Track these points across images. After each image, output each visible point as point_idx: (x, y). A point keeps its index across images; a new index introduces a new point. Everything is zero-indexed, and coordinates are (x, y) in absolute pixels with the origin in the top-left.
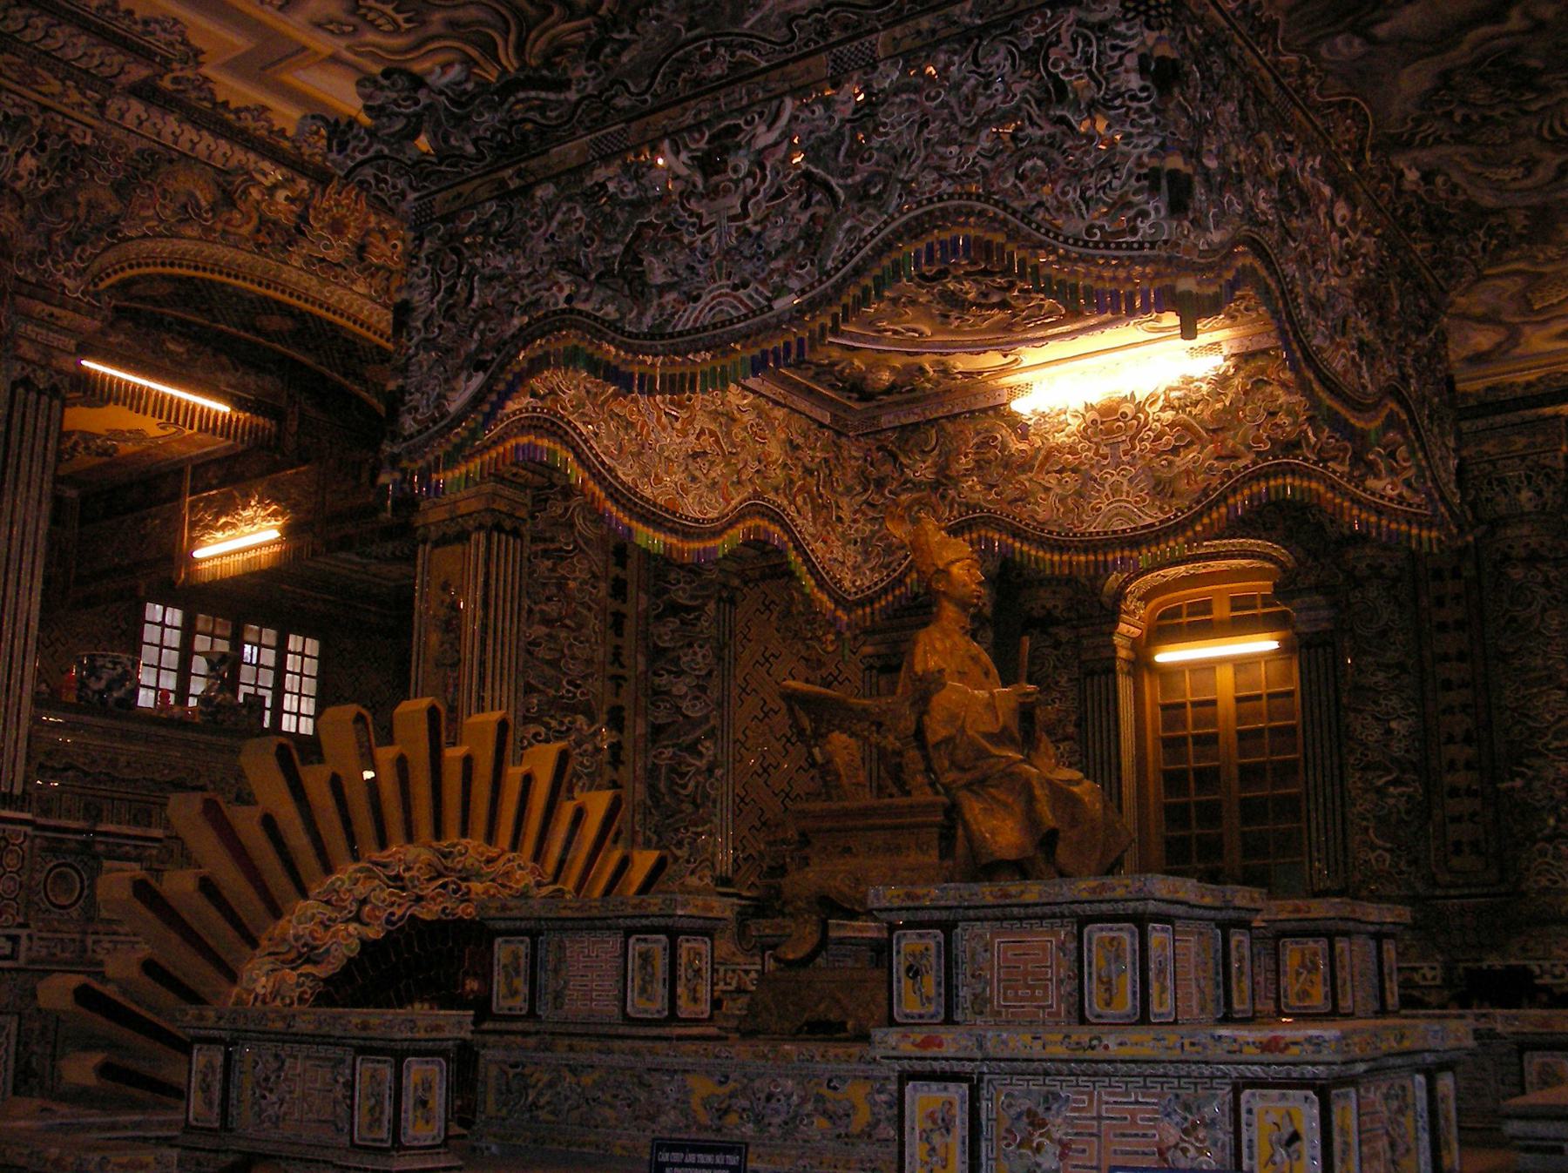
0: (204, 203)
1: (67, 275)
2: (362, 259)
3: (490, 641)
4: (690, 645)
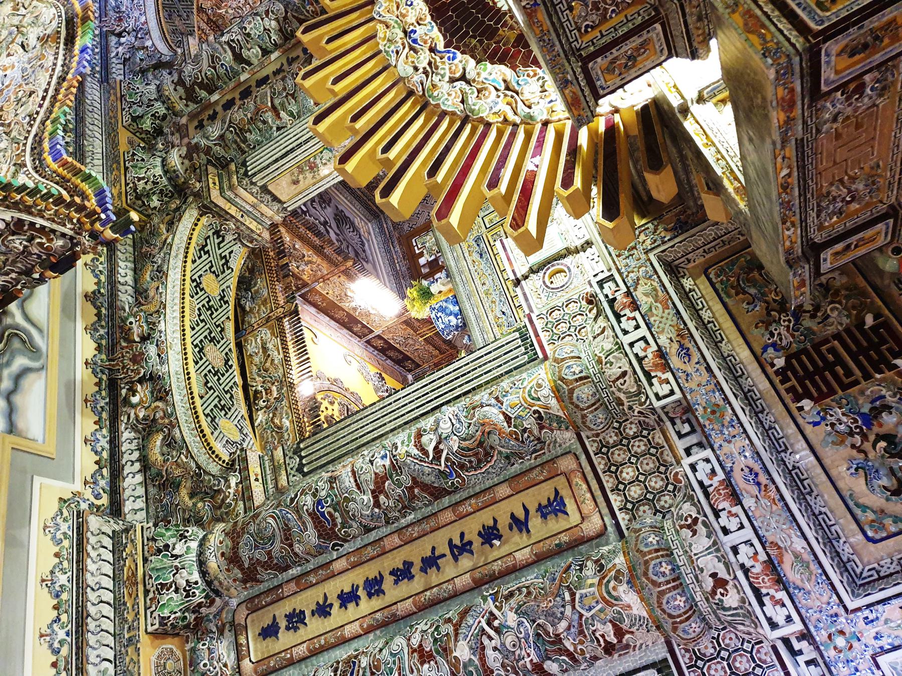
0: (161, 437)
1: (230, 488)
2: (149, 334)
3: (304, 138)
4: (249, 35)
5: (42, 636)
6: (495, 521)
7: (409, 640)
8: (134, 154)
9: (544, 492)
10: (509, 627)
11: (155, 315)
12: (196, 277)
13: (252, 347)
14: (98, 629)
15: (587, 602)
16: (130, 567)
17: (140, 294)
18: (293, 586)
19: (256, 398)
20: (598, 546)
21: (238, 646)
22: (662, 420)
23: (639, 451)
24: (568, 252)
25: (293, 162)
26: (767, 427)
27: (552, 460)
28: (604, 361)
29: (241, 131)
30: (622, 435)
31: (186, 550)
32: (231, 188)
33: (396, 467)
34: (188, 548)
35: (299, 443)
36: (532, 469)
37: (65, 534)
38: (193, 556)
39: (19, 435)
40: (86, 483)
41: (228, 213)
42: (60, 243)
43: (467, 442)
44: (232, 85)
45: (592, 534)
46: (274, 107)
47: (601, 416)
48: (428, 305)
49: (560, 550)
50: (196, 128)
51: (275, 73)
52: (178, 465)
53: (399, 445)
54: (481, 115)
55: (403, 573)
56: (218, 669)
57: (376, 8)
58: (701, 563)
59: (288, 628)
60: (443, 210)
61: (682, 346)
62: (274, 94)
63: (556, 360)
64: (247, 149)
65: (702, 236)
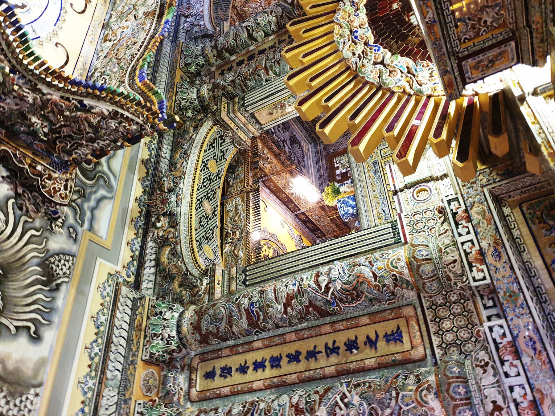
0: (169, 249)
1: (202, 285)
2: (173, 189)
3: (280, 88)
4: (259, 24)
5: (86, 348)
6: (356, 338)
7: (291, 399)
8: (182, 85)
9: (391, 326)
10: (353, 405)
11: (178, 179)
12: (205, 160)
13: (229, 206)
14: (116, 351)
15: (406, 400)
16: (139, 320)
17: (172, 165)
18: (227, 352)
19: (226, 236)
20: (419, 366)
21: (191, 379)
22: (475, 295)
23: (456, 312)
24: (432, 179)
25: (271, 102)
26: (547, 313)
27: (399, 308)
28: (443, 251)
29: (245, 80)
30: (447, 299)
31: (172, 316)
32: (234, 112)
33: (301, 292)
34: (173, 316)
35: (246, 267)
36: (384, 311)
37: (108, 293)
38: (174, 321)
39: (94, 233)
40: (124, 267)
41: (230, 127)
42: (135, 127)
43: (347, 286)
44: (244, 52)
45: (416, 358)
46: (266, 68)
47: (435, 285)
48: (337, 198)
49: (395, 364)
50: (219, 74)
51: (270, 48)
52: (176, 267)
53: (305, 279)
54: (389, 86)
55: (294, 358)
56: (177, 390)
57: (336, 15)
58: (486, 392)
59: (221, 376)
60: (356, 141)
61: (496, 250)
62: (268, 60)
63: (413, 245)
64: (246, 90)
65: (521, 182)
